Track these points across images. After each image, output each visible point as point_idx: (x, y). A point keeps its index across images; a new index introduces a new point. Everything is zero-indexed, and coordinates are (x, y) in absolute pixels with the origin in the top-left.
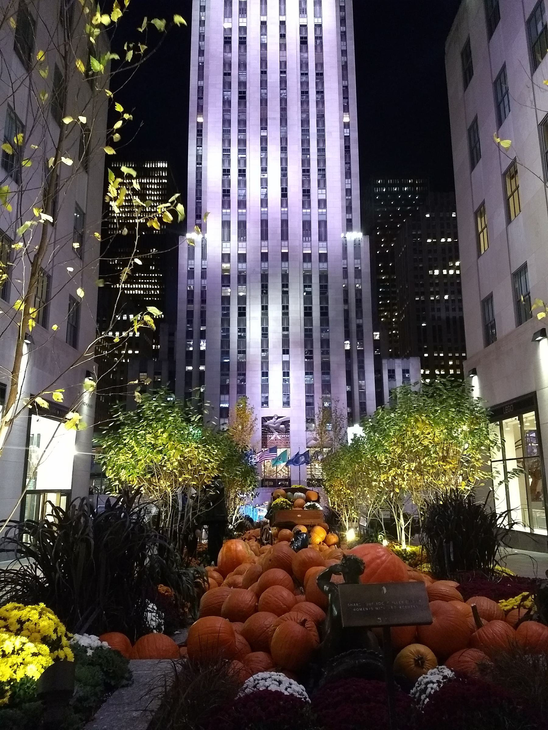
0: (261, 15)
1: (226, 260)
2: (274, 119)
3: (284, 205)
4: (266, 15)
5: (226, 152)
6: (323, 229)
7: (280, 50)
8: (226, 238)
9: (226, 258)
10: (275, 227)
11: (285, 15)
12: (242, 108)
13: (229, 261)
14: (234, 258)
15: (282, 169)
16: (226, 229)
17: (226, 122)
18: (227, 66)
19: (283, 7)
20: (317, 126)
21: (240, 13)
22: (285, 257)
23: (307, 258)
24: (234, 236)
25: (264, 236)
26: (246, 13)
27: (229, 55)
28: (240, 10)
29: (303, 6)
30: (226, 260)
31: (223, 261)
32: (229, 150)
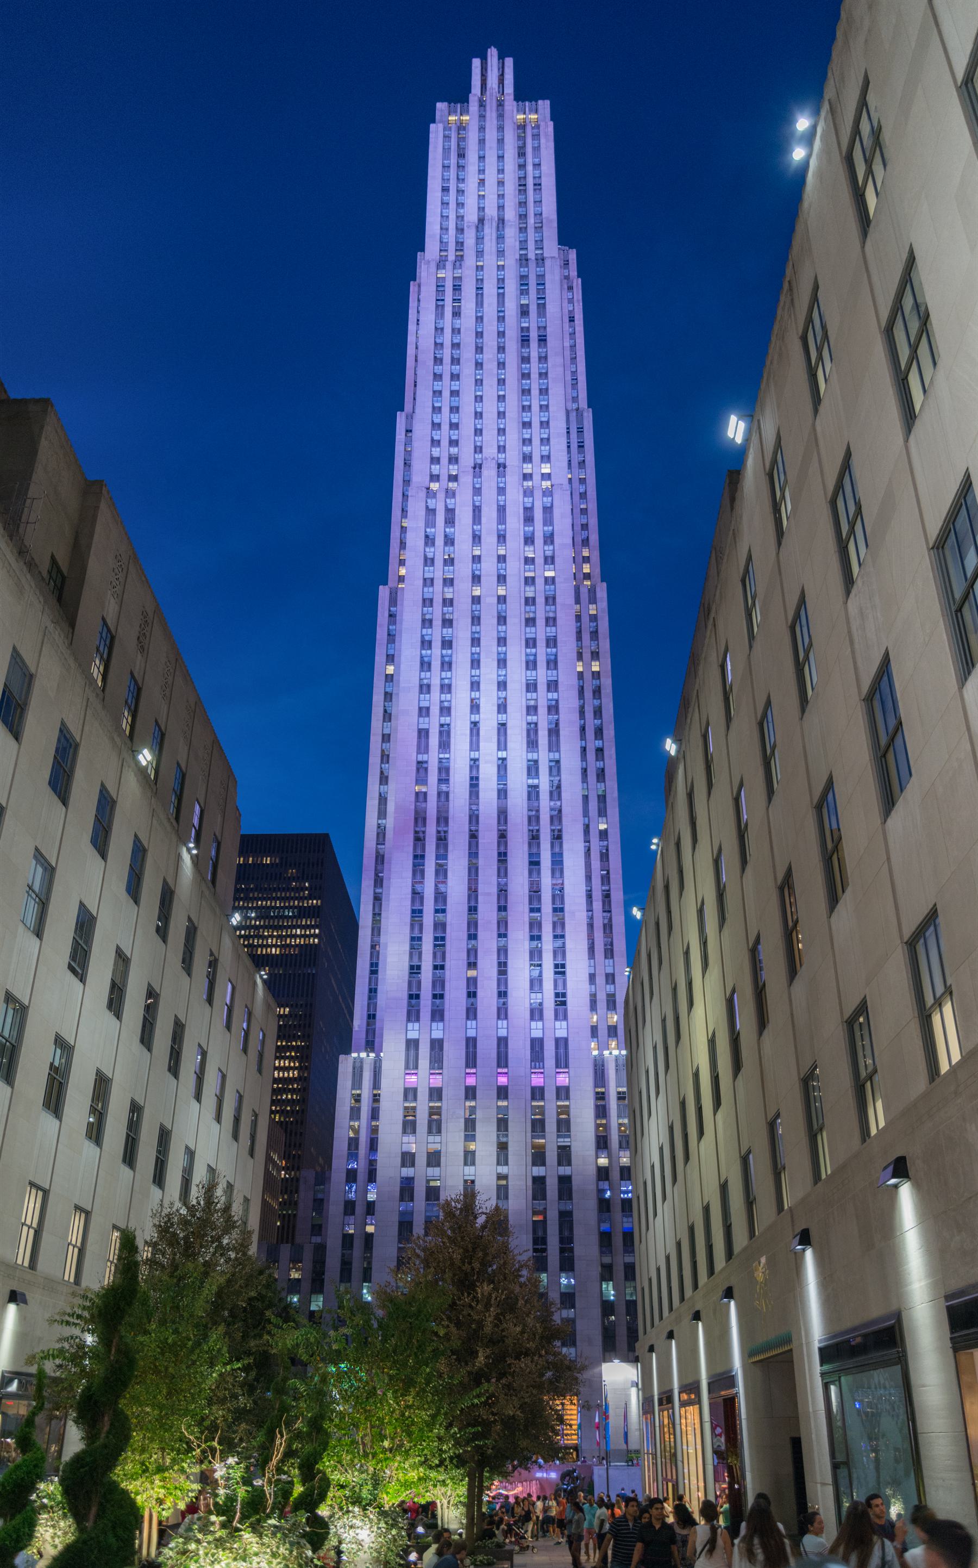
0: (471, 750)
1: (410, 1096)
2: (489, 894)
3: (502, 1016)
4: (478, 750)
5: (416, 941)
6: (562, 1051)
7: (499, 798)
8: (411, 1064)
9: (409, 1093)
10: (487, 1050)
11: (506, 749)
12: (441, 878)
13: (415, 1099)
14: (423, 1095)
15: (500, 964)
16: (412, 1052)
17: (417, 896)
18: (420, 821)
19: (502, 739)
20: (553, 903)
21: (440, 747)
22: (503, 1092)
23: (538, 1093)
24: (424, 1062)
25: (471, 1060)
26: (449, 747)
27: (423, 805)
28: (440, 742)
29: (532, 736)
30: (410, 1096)
31: (406, 1098)
32: (420, 939)
